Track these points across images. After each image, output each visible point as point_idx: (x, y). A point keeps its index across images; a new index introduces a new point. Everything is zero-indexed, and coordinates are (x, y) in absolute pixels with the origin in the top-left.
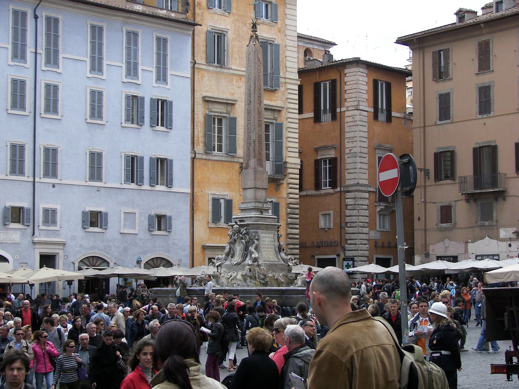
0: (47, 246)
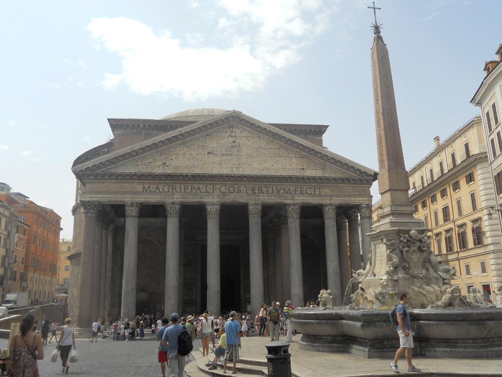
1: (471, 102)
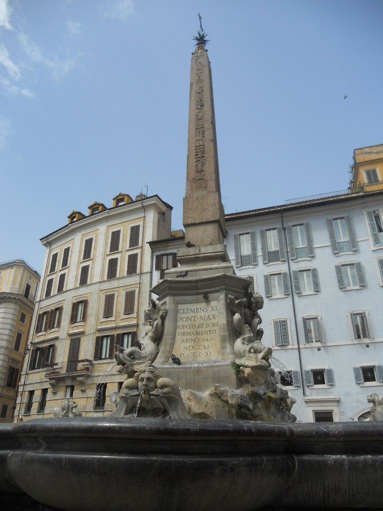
0: (319, 404)
1: (41, 240)
